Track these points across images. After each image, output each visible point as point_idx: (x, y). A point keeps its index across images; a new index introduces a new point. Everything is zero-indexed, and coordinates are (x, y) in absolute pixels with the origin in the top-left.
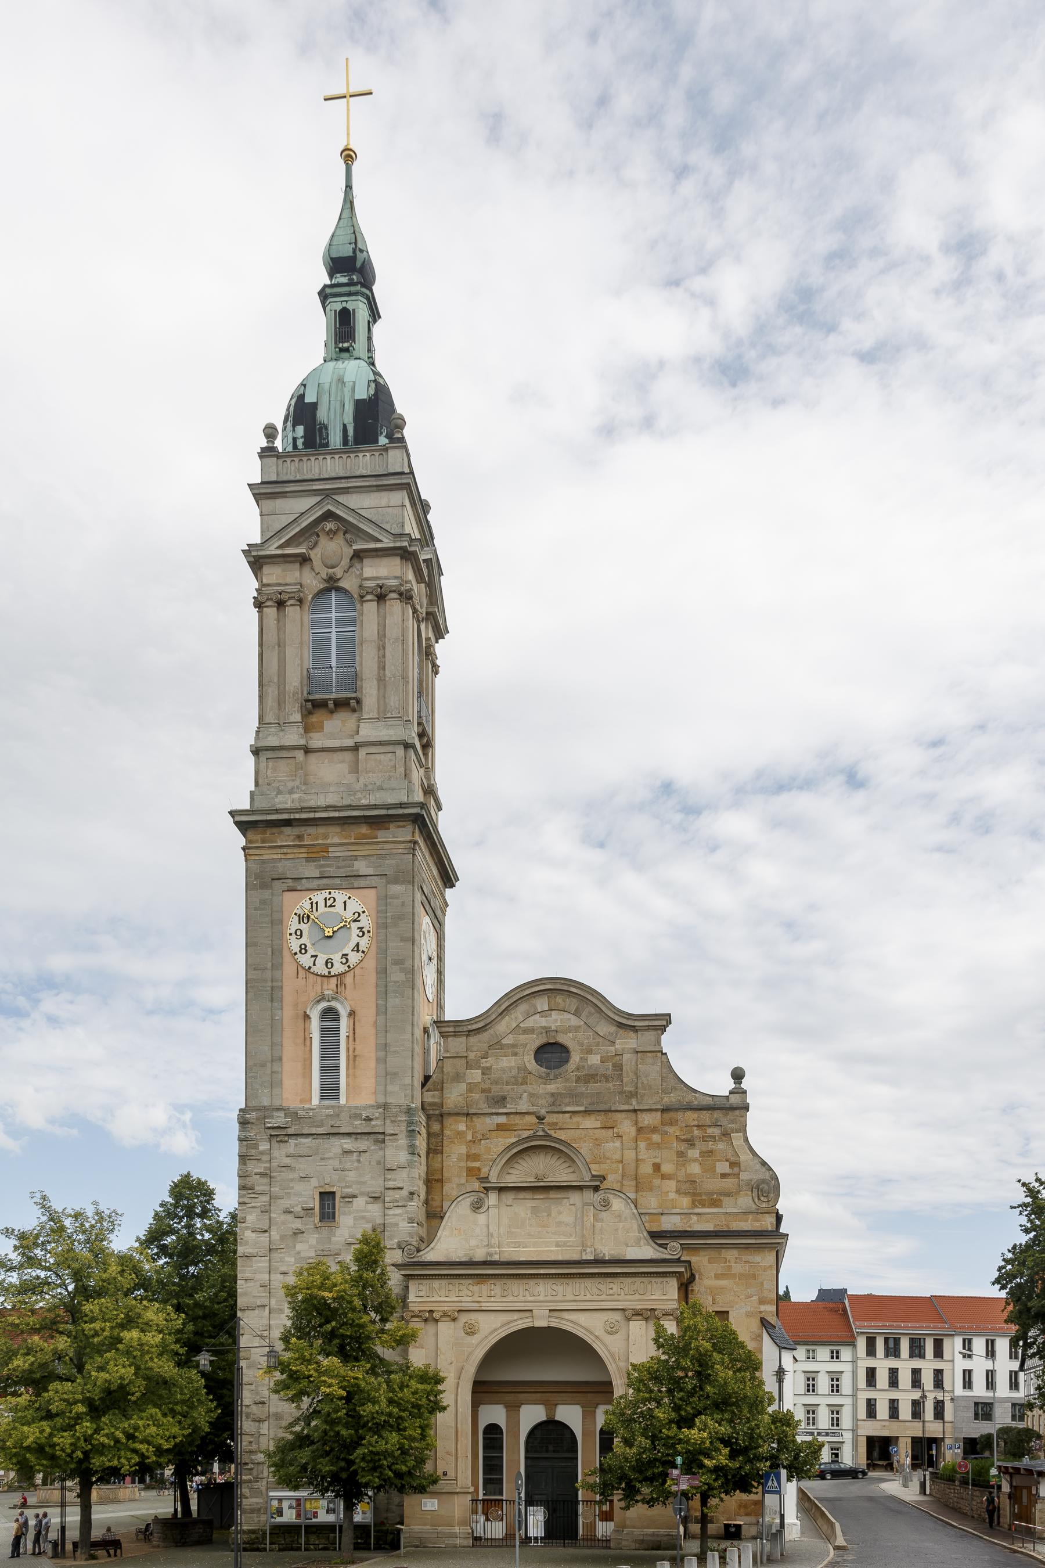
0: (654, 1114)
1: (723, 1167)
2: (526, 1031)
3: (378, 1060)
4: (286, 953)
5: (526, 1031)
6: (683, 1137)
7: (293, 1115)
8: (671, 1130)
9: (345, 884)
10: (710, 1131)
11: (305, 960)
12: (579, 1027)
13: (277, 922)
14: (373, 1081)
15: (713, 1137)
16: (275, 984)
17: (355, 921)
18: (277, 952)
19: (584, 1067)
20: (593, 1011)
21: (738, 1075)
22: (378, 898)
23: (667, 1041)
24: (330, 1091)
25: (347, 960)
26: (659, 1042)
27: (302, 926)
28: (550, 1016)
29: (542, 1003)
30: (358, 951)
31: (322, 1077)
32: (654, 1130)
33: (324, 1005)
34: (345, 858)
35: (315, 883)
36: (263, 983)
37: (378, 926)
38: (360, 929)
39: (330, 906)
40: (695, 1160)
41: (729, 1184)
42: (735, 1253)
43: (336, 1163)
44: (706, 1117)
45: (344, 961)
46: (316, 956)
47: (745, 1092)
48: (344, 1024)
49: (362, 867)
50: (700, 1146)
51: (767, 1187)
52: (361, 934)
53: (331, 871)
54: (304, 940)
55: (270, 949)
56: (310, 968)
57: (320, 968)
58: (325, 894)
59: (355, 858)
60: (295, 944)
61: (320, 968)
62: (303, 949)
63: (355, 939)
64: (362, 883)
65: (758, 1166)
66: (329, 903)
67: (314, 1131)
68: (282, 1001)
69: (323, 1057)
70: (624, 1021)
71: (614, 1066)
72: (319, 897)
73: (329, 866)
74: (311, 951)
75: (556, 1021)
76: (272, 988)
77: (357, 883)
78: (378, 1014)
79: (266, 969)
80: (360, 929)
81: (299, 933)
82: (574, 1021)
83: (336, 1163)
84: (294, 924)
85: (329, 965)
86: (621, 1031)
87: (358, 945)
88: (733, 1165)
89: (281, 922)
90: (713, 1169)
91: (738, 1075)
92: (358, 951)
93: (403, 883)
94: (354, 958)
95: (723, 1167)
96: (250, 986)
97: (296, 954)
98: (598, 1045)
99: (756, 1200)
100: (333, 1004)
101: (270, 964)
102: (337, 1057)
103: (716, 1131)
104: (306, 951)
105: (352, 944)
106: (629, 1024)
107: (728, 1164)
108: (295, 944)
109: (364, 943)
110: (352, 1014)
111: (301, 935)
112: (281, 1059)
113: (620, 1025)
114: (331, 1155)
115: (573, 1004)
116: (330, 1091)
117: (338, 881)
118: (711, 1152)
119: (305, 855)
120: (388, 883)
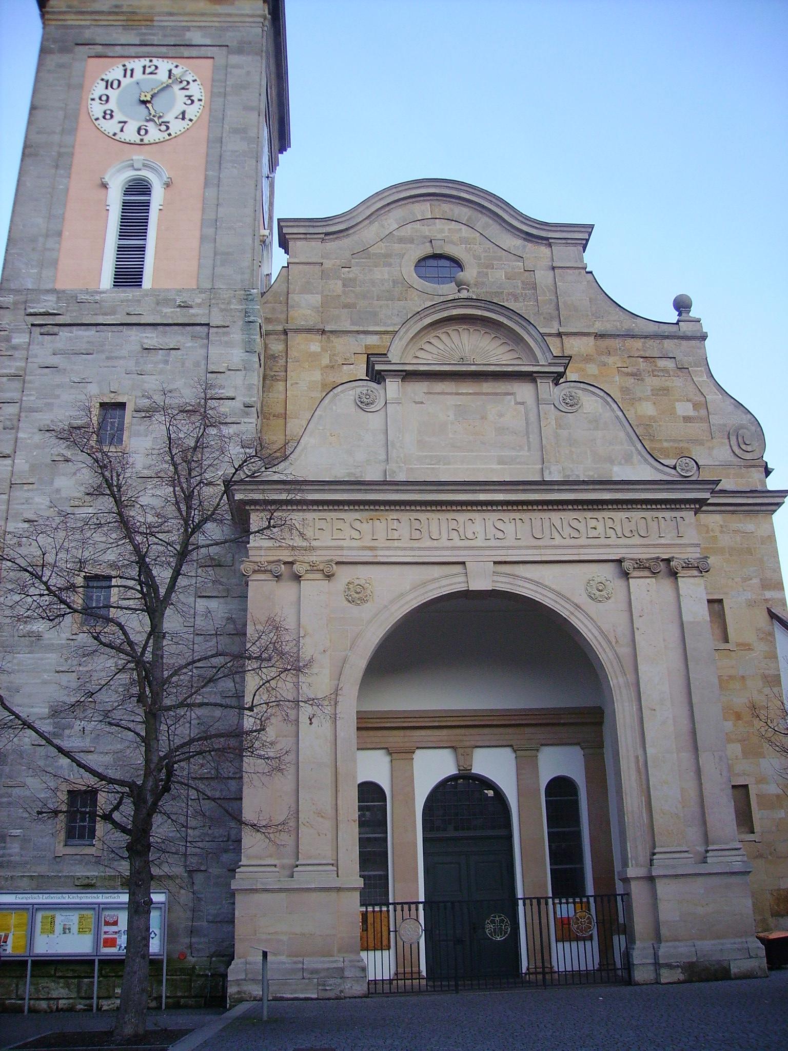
0: (585, 339)
1: (684, 409)
2: (401, 240)
3: (203, 238)
4: (83, 117)
5: (401, 240)
6: (629, 370)
7: (74, 299)
8: (610, 360)
9: (172, 51)
10: (662, 363)
11: (110, 127)
12: (474, 238)
13: (78, 87)
14: (195, 263)
15: (665, 370)
16: (63, 150)
17: (183, 89)
18: (72, 118)
19: (483, 283)
20: (491, 222)
21: (682, 305)
22: (215, 69)
23: (592, 258)
24: (128, 276)
25: (168, 128)
26: (582, 259)
27: (110, 92)
28: (435, 224)
29: (423, 209)
30: (183, 119)
31: (118, 259)
32: (588, 359)
33: (130, 174)
34: (173, 28)
35: (132, 51)
36: (46, 149)
37: (213, 95)
38: (189, 97)
39: (151, 73)
40: (647, 399)
41: (696, 429)
42: (717, 518)
43: (131, 365)
44: (653, 348)
45: (163, 128)
46: (125, 122)
47: (698, 321)
48: (157, 198)
49: (196, 37)
50: (651, 382)
51: (747, 437)
52: (189, 102)
53: (155, 40)
54: (112, 105)
55: (61, 113)
56: (115, 134)
57: (130, 134)
58: (145, 61)
59: (188, 29)
60: (97, 109)
61: (130, 134)
62: (108, 115)
63: (179, 107)
64: (194, 52)
65: (730, 408)
66: (148, 70)
67: (100, 319)
68: (70, 169)
69: (123, 234)
70: (534, 232)
71: (523, 282)
72: (137, 65)
73: (153, 35)
74: (118, 116)
75: (442, 231)
76: (60, 155)
77: (186, 52)
78: (206, 185)
79: (54, 133)
80: (189, 97)
81: (104, 98)
82: (465, 232)
83: (131, 365)
84: (99, 89)
85: (143, 132)
86: (529, 245)
87: (184, 113)
88: (696, 406)
89: (81, 86)
90: (672, 411)
91: (682, 305)
92: (183, 119)
93: (249, 54)
94: (177, 127)
95: (684, 409)
96: (29, 151)
97: (97, 119)
98: (500, 259)
99: (737, 451)
100: (144, 173)
101: (58, 129)
102: (143, 234)
103: (670, 364)
104: (112, 116)
105: (177, 111)
106: (538, 234)
107: (690, 406)
108: (97, 109)
109: (193, 111)
110: (167, 185)
111: (107, 101)
112: (60, 234)
113: (529, 237)
114: (124, 353)
115: (463, 212)
116: (128, 276)
117: (164, 50)
118: (667, 389)
119: (124, 23)
120: (229, 53)
